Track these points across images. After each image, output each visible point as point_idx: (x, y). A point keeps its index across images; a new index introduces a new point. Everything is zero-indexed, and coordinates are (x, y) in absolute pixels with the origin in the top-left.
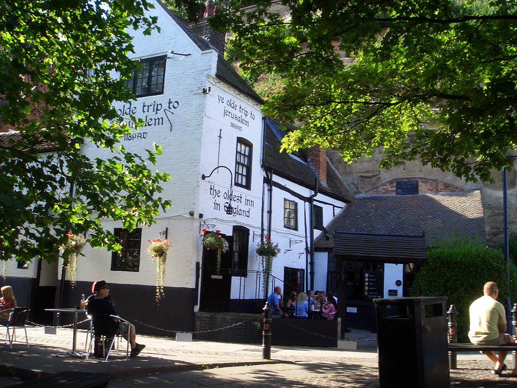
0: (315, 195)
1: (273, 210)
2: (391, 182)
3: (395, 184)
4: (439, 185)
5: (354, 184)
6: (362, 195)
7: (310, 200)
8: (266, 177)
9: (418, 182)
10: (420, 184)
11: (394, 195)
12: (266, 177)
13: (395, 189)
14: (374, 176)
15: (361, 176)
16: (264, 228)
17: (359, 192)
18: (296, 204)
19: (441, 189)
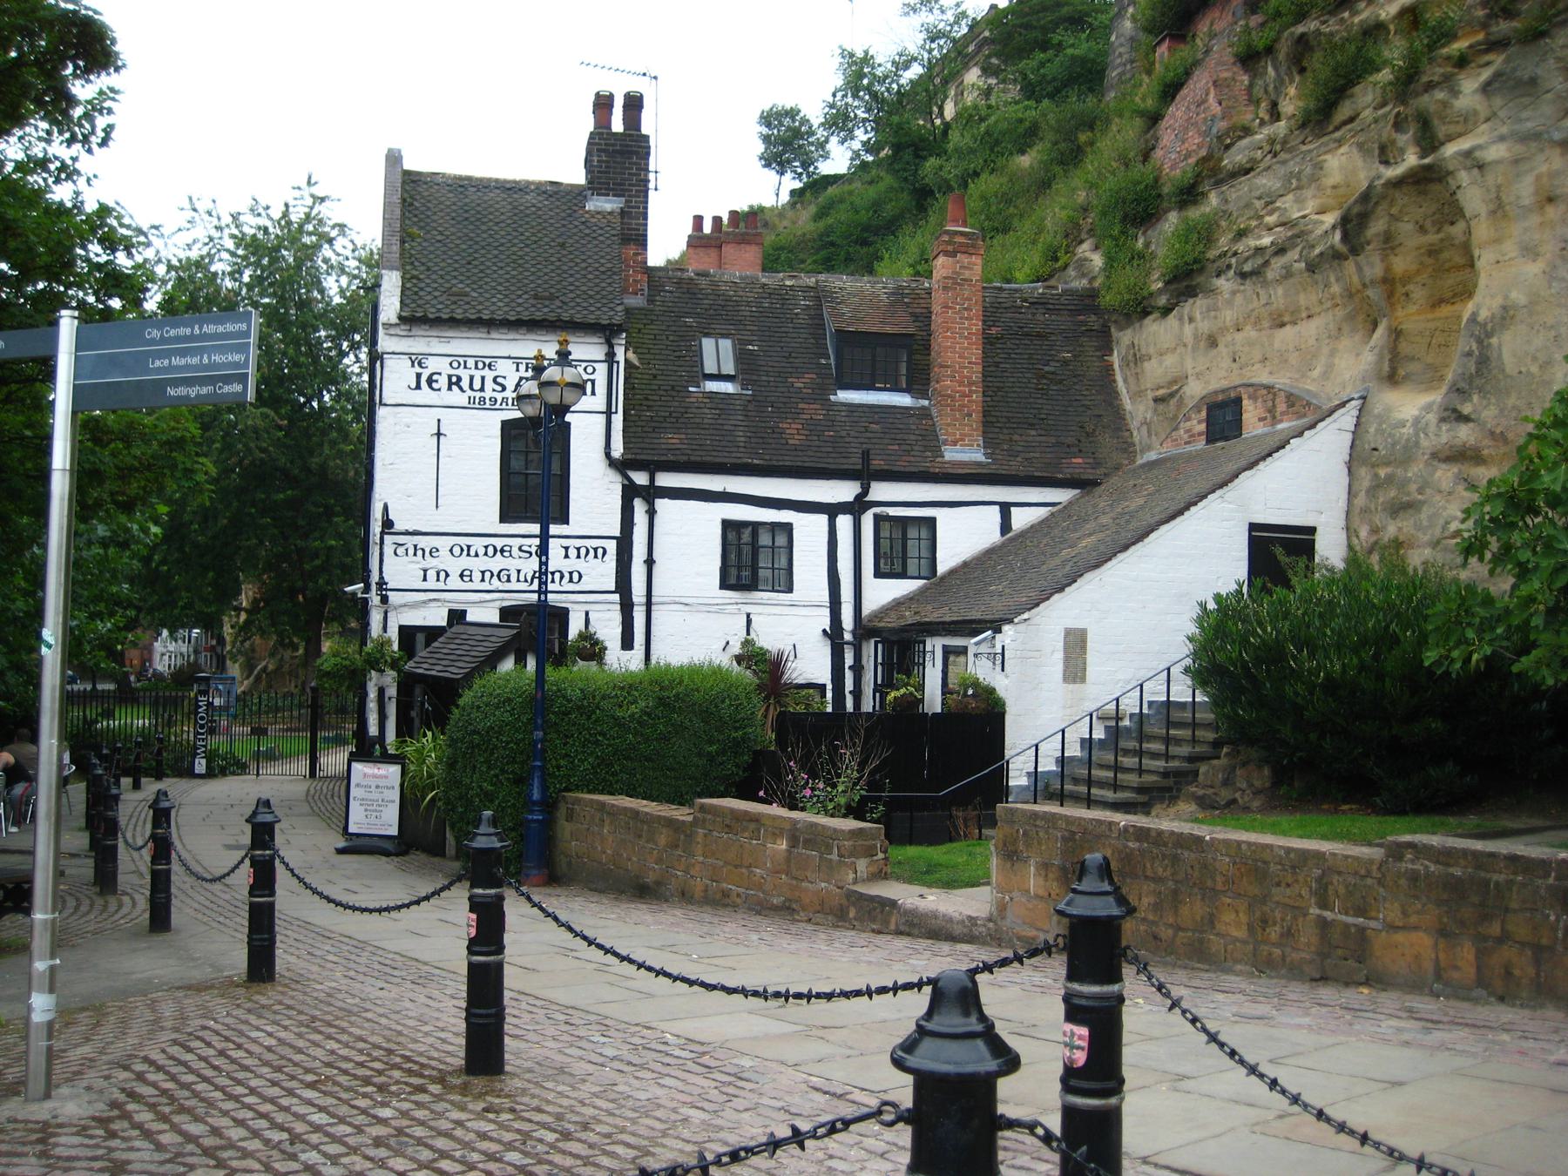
0: (865, 491)
1: (656, 556)
2: (1197, 408)
3: (1204, 414)
4: (1278, 400)
5: (1145, 423)
6: (1152, 456)
7: (857, 508)
8: (626, 482)
9: (1238, 401)
10: (1245, 402)
11: (1201, 444)
12: (626, 482)
13: (1203, 427)
14: (1172, 395)
15: (1156, 400)
16: (635, 599)
17: (1149, 448)
18: (788, 528)
19: (1283, 414)
